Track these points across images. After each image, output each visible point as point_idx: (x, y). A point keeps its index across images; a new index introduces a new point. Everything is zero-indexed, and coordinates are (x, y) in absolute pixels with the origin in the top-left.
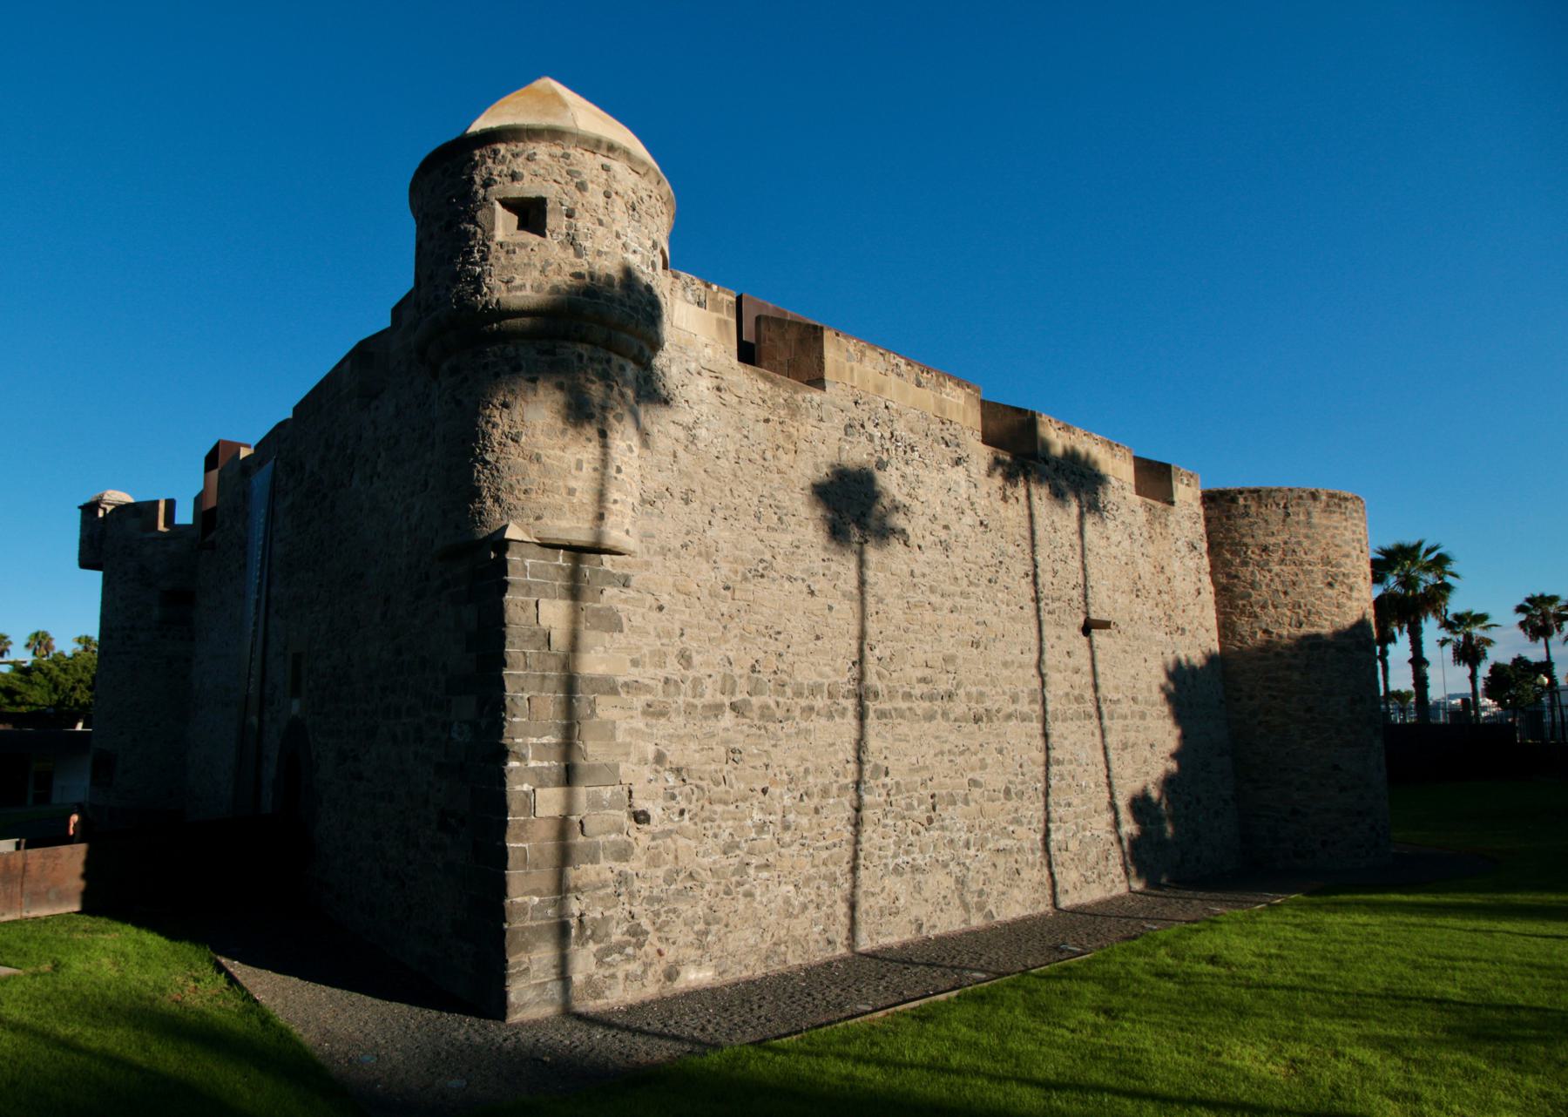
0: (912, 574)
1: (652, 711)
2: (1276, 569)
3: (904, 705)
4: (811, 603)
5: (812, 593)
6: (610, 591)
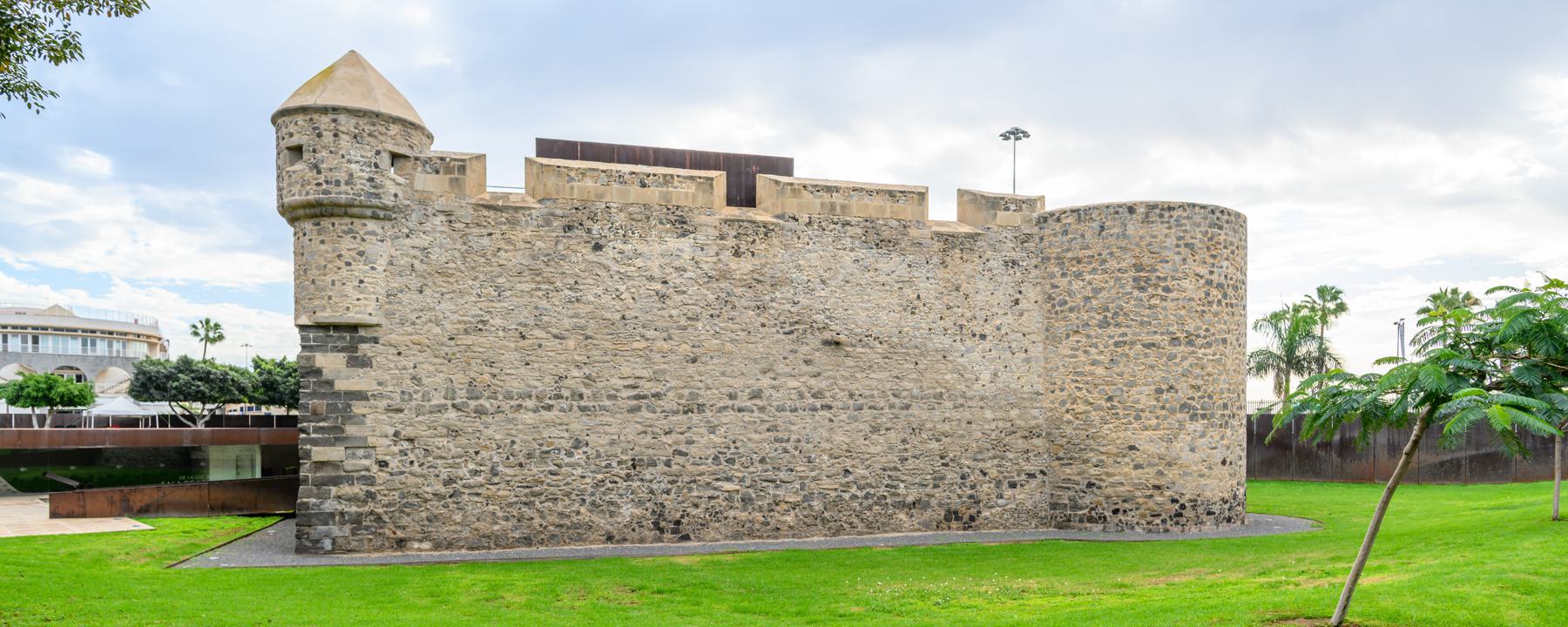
0: (623, 317)
1: (389, 409)
2: (1088, 277)
3: (608, 403)
4: (522, 343)
5: (523, 337)
6: (363, 346)
